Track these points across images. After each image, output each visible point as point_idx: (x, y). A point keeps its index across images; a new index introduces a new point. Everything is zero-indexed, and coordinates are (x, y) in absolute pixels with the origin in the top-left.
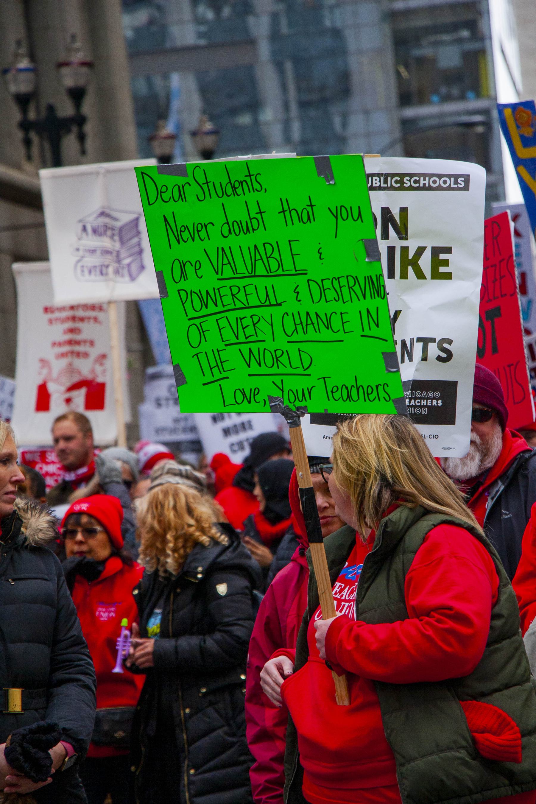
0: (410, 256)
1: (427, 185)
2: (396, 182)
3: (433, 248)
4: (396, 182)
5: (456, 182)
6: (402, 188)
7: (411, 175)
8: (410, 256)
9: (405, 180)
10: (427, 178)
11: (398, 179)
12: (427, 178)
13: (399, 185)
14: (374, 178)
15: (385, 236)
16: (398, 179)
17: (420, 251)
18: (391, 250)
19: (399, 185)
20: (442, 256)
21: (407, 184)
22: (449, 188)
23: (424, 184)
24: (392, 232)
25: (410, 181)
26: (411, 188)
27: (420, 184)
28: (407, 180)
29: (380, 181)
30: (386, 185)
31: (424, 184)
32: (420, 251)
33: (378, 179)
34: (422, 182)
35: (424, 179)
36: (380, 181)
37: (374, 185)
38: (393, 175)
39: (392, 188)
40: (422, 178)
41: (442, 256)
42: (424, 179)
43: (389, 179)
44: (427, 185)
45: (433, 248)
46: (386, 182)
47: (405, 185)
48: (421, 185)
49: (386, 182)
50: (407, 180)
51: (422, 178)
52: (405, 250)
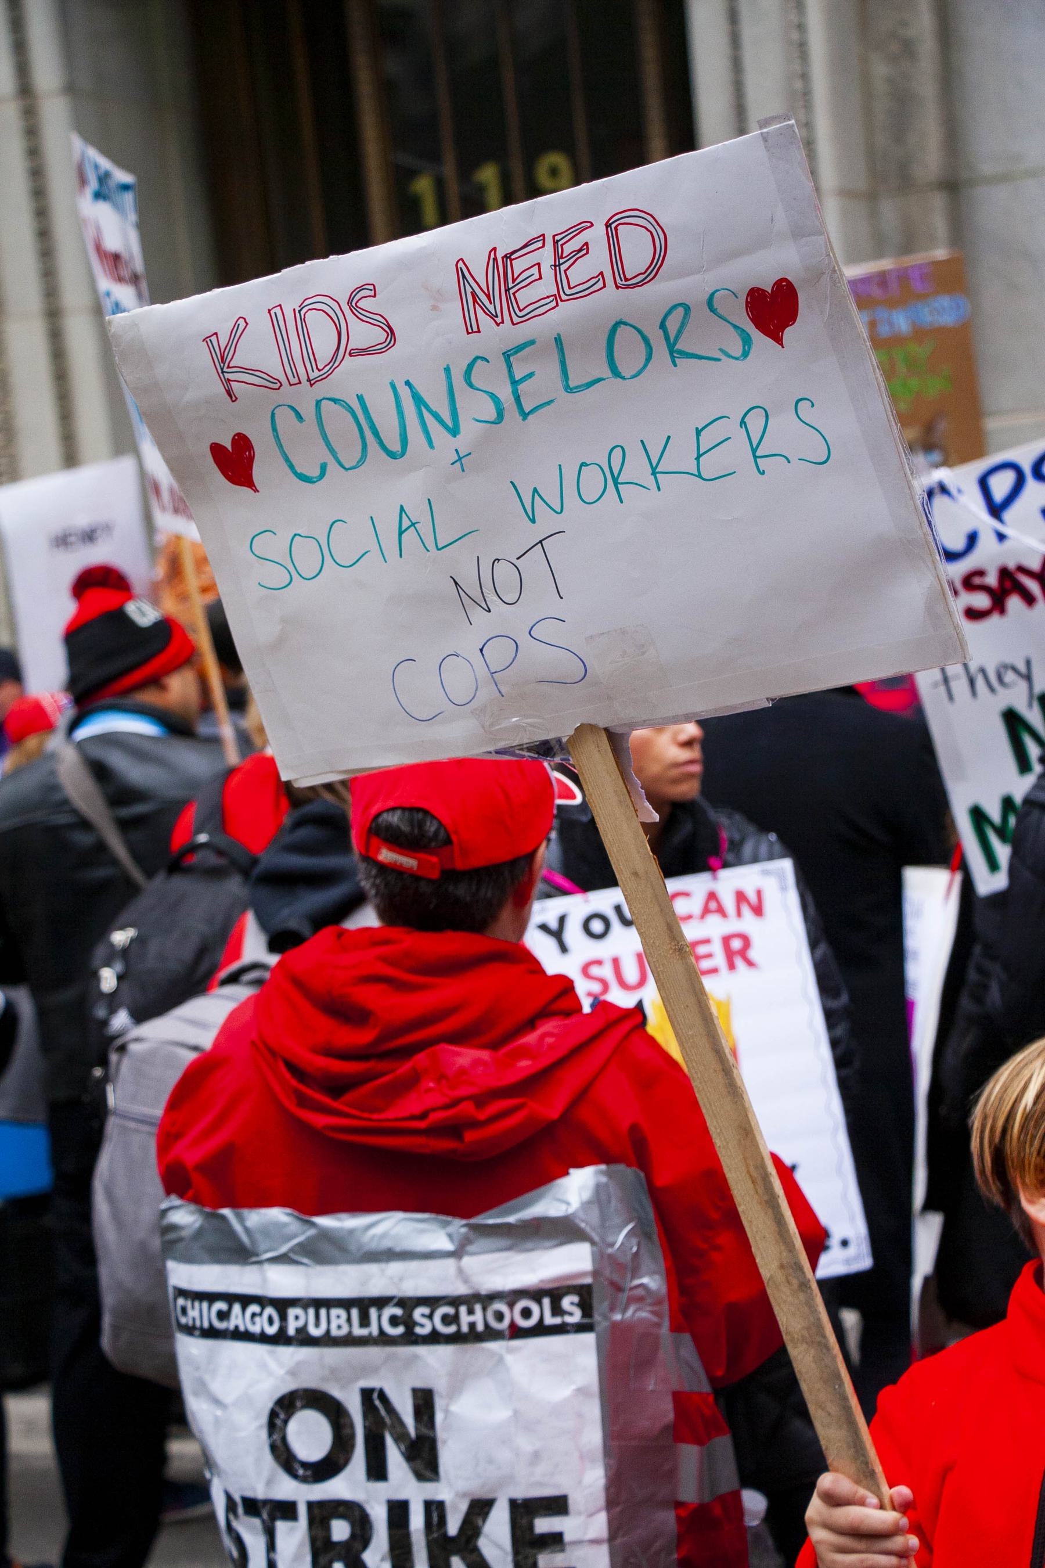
0: (453, 1528)
1: (480, 1327)
2: (394, 1321)
3: (513, 1503)
4: (394, 1321)
5: (557, 1310)
6: (411, 1338)
7: (432, 1302)
8: (453, 1528)
9: (419, 1313)
10: (478, 1308)
11: (398, 1311)
12: (478, 1308)
13: (400, 1330)
14: (334, 1312)
15: (377, 1470)
16: (398, 1311)
17: (480, 1508)
18: (398, 1511)
19: (400, 1330)
20: (543, 1525)
21: (422, 1326)
22: (541, 1330)
23: (472, 1326)
24: (394, 1456)
25: (430, 1317)
26: (434, 1338)
27: (459, 1326)
28: (423, 1315)
29: (349, 1320)
30: (364, 1332)
31: (472, 1326)
32: (480, 1508)
33: (342, 1313)
34: (465, 1319)
35: (471, 1312)
36: (349, 1320)
37: (335, 1332)
38: (381, 1302)
39: (383, 1339)
40: (463, 1310)
41: (543, 1525)
42: (471, 1312)
43: (373, 1312)
44: (480, 1327)
45: (513, 1503)
46: (365, 1322)
47: (418, 1330)
48: (465, 1329)
49: (365, 1322)
50: (423, 1315)
51: (463, 1310)
52: (435, 1510)
